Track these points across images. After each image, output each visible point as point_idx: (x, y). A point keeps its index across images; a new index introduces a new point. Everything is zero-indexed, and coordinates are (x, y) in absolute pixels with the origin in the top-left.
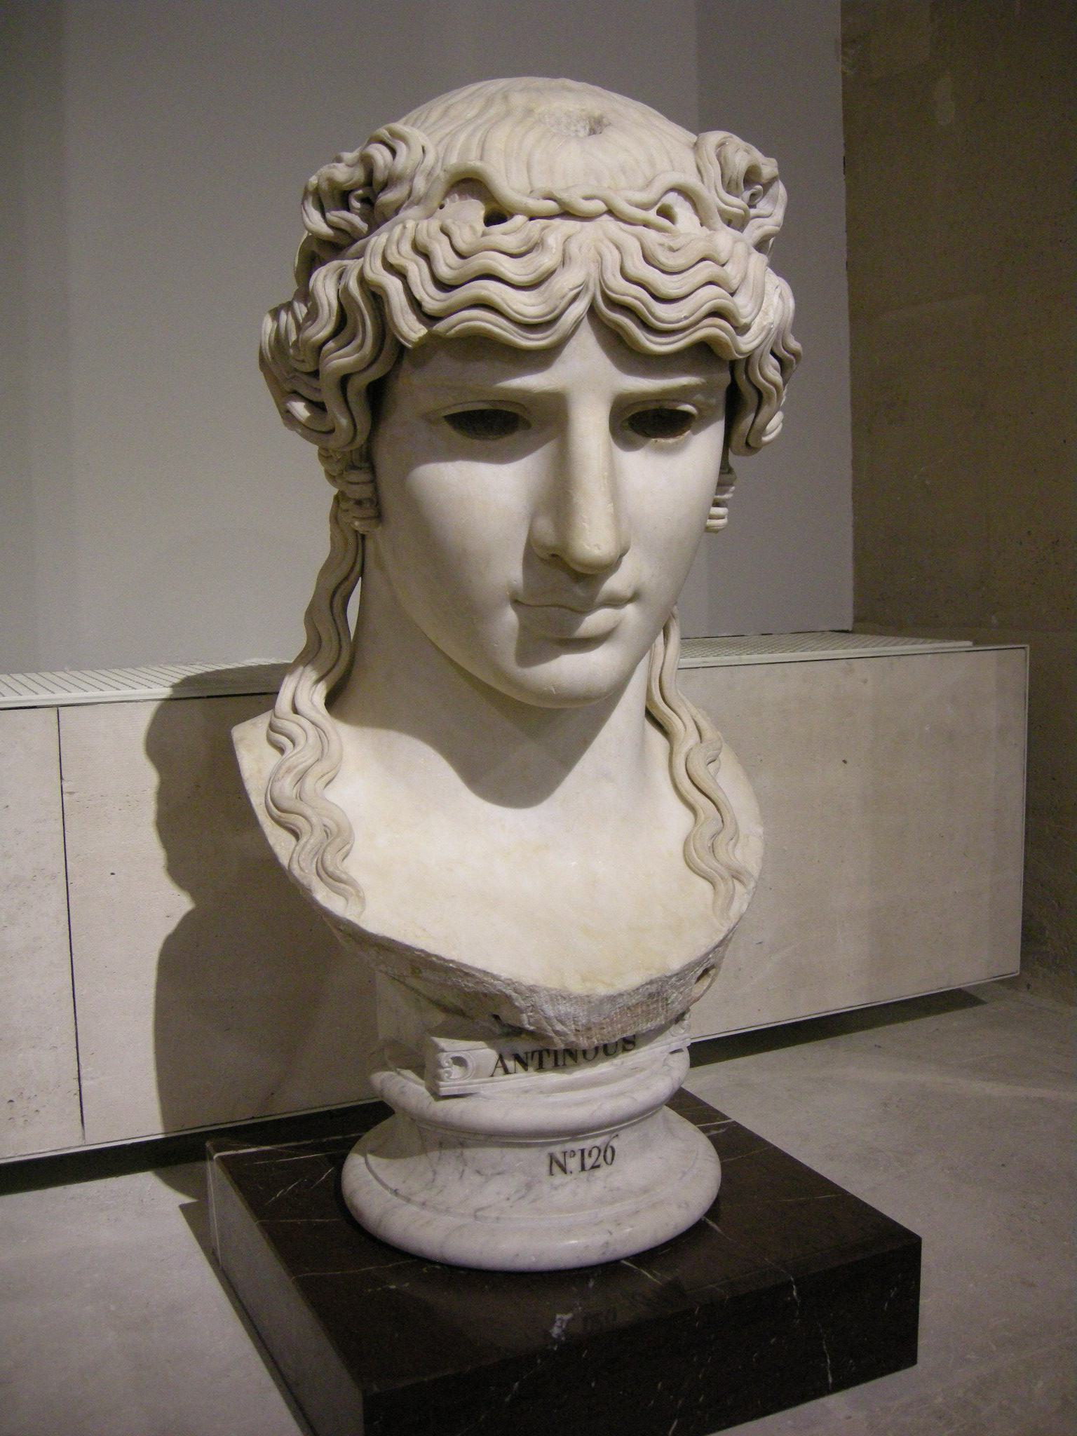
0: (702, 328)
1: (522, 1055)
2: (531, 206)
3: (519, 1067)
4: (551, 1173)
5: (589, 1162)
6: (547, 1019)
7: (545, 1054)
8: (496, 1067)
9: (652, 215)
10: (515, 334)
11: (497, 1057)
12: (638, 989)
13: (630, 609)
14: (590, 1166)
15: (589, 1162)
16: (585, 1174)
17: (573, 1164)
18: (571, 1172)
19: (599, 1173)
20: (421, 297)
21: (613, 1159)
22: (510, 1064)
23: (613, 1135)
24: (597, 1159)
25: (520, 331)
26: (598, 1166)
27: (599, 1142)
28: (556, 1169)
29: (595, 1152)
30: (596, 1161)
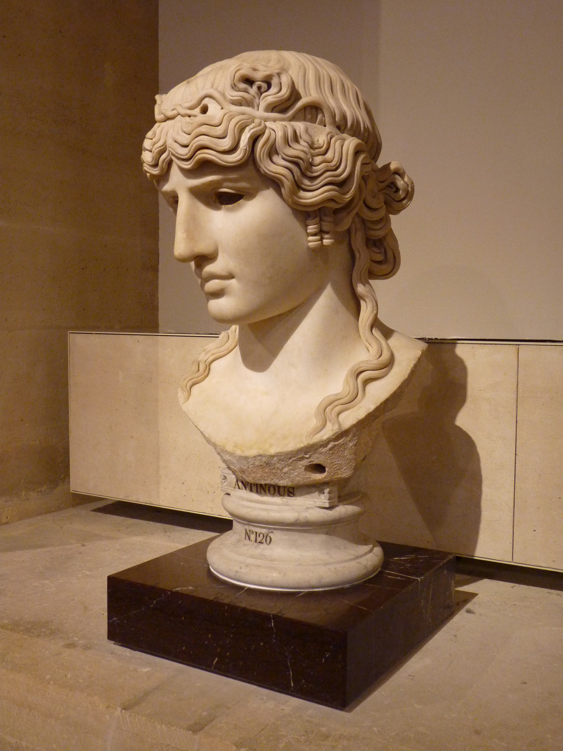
0: (198, 155)
1: (245, 483)
3: (243, 488)
4: (245, 539)
5: (259, 539)
7: (253, 486)
8: (235, 484)
9: (197, 111)
11: (236, 480)
12: (254, 457)
13: (233, 282)
14: (259, 541)
15: (259, 539)
16: (256, 544)
17: (253, 537)
18: (251, 541)
19: (262, 546)
21: (270, 543)
22: (240, 484)
23: (270, 531)
24: (262, 539)
25: (152, 168)
26: (262, 543)
27: (264, 531)
28: (247, 537)
29: (261, 535)
30: (261, 540)
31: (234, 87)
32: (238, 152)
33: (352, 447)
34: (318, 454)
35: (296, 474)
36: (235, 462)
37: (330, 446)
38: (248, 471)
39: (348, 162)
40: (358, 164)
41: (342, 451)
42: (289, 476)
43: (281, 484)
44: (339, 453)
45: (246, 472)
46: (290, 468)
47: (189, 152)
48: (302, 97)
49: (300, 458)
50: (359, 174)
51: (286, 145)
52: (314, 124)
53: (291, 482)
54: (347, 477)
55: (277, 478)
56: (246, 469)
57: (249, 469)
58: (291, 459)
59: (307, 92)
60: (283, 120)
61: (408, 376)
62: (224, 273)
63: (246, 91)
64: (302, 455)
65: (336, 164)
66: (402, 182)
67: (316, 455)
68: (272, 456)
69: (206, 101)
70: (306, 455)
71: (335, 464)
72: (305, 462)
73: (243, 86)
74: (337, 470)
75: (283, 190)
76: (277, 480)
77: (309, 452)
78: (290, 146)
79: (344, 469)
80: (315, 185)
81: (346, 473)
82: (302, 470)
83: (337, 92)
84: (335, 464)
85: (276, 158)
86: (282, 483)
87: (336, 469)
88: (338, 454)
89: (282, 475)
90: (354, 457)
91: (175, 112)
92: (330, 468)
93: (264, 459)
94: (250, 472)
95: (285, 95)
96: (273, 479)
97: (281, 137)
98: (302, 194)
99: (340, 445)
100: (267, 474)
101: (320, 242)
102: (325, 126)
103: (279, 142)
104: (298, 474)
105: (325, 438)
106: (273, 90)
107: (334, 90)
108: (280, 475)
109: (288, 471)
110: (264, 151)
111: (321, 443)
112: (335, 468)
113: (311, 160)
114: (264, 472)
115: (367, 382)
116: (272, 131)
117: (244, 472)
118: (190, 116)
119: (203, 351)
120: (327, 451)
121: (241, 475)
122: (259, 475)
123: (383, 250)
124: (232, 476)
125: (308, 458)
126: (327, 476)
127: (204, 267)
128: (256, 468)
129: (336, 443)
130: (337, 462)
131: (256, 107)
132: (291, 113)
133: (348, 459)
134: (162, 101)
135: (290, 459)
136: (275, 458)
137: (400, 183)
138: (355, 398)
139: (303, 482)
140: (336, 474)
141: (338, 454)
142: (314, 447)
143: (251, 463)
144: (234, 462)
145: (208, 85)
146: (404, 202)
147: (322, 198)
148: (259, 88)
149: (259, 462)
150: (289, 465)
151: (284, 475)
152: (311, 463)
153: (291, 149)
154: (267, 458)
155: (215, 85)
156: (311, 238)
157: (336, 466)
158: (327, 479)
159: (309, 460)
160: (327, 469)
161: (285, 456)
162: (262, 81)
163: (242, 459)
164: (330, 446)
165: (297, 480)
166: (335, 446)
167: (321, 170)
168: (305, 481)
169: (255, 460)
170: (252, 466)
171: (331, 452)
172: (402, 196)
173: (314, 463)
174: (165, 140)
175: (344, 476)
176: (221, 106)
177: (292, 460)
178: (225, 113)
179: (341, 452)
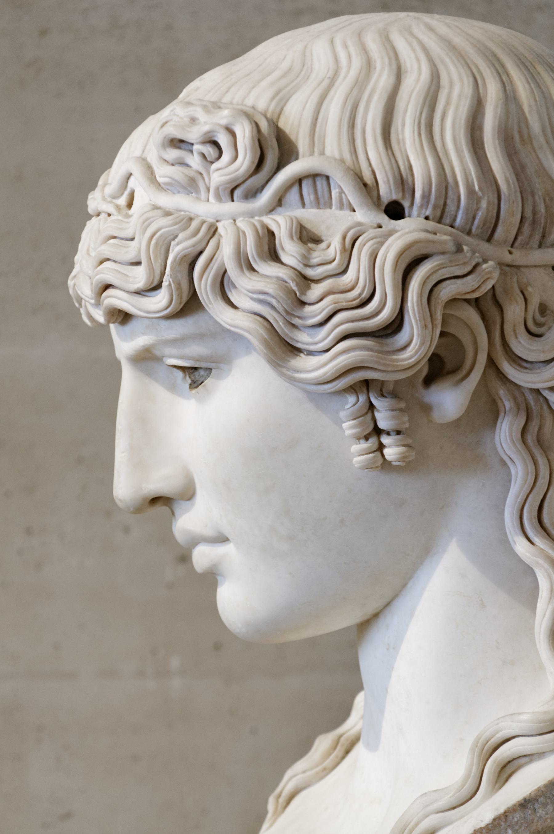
40: (414, 286)
50: (416, 308)
51: (242, 269)
52: (329, 210)
78: (252, 269)
83: (403, 125)
102: (354, 211)
106: (226, 157)
147: (334, 367)
148: (204, 156)
153: (253, 276)
162: (204, 143)
167: (323, 310)
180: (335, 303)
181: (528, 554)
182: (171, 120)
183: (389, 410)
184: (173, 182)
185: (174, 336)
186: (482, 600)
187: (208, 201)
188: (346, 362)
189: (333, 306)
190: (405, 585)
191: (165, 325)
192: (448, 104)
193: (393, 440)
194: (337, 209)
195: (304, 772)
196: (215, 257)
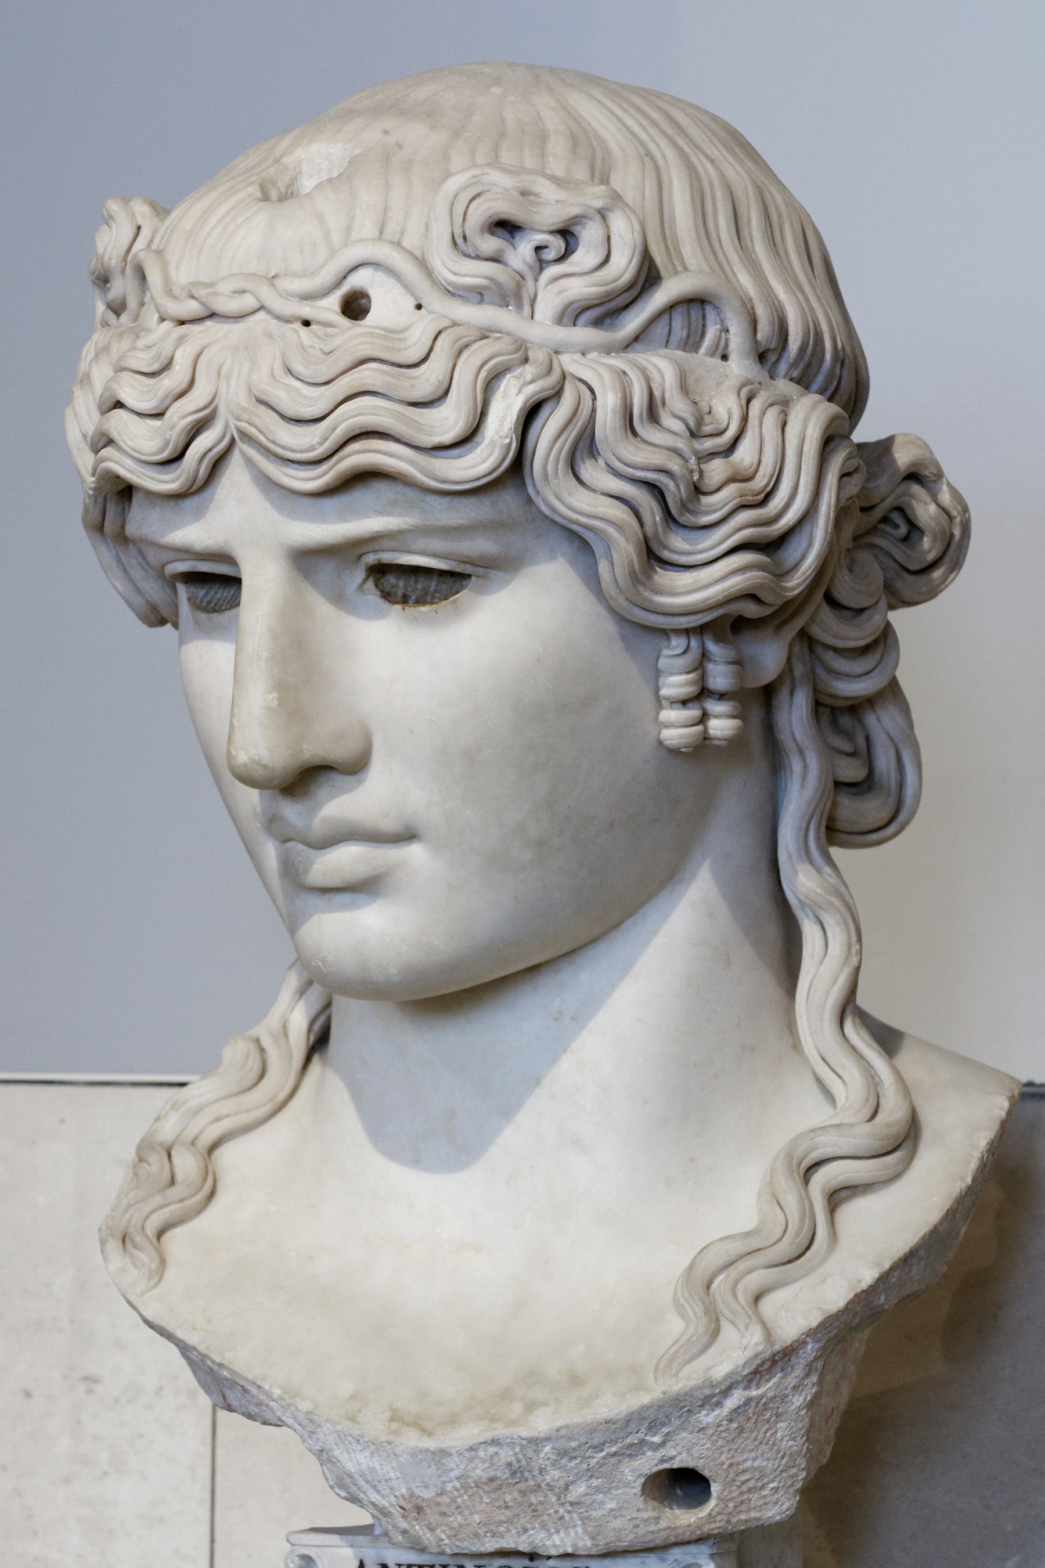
2: (169, 311)
6: (350, 1476)
10: (142, 476)
12: (471, 1449)
13: (415, 852)
20: (86, 430)
31: (459, 244)
32: (479, 449)
33: (800, 1408)
34: (691, 1433)
35: (611, 1505)
36: (392, 1475)
37: (732, 1402)
38: (439, 1504)
39: (802, 476)
41: (768, 1421)
42: (586, 1514)
43: (555, 1546)
44: (759, 1431)
45: (429, 1512)
46: (595, 1482)
47: (321, 444)
48: (663, 272)
49: (631, 1445)
52: (695, 354)
53: (593, 1538)
54: (778, 1518)
55: (544, 1526)
56: (429, 1500)
57: (445, 1499)
58: (602, 1450)
59: (672, 251)
60: (608, 349)
61: (974, 1179)
62: (389, 825)
63: (496, 259)
64: (640, 1435)
65: (766, 486)
66: (933, 508)
67: (684, 1434)
68: (536, 1442)
69: (359, 280)
70: (655, 1435)
71: (744, 1471)
72: (649, 1463)
73: (491, 244)
74: (749, 1491)
75: (603, 568)
76: (542, 1535)
77: (664, 1425)
78: (634, 433)
79: (772, 1489)
80: (701, 552)
81: (776, 1503)
82: (634, 1491)
84: (744, 1471)
85: (589, 471)
86: (558, 1543)
87: (744, 1488)
88: (754, 1435)
89: (561, 1511)
90: (805, 1447)
91: (248, 302)
92: (728, 1484)
93: (506, 1455)
94: (444, 1510)
95: (622, 276)
96: (526, 1530)
97: (614, 411)
98: (664, 577)
99: (764, 1400)
100: (507, 1513)
101: (700, 728)
102: (725, 357)
103: (606, 425)
104: (620, 1508)
105: (720, 1372)
106: (585, 257)
107: (745, 233)
108: (556, 1512)
109: (586, 1494)
110: (561, 450)
111: (707, 1392)
112: (743, 1483)
113: (696, 477)
114: (497, 1504)
115: (837, 1197)
116: (583, 388)
117: (419, 1509)
118: (307, 323)
119: (171, 1108)
120: (721, 1421)
121: (404, 1525)
122: (477, 1518)
123: (861, 741)
124: (338, 1550)
125: (657, 1447)
126: (714, 1513)
127: (320, 806)
128: (471, 1491)
129: (754, 1393)
130: (750, 1462)
131: (527, 309)
132: (633, 322)
133: (783, 1457)
134: (139, 228)
135: (599, 1447)
136: (548, 1448)
137: (925, 511)
138: (808, 1248)
139: (632, 1536)
140: (744, 1507)
141: (754, 1435)
142: (682, 1404)
143: (453, 1474)
144: (387, 1477)
145: (366, 227)
146: (937, 574)
147: (724, 591)
148: (538, 249)
149: (486, 1465)
150: (591, 1473)
151: (569, 1512)
152: (667, 1466)
154: (518, 1449)
155: (391, 229)
156: (670, 714)
157: (747, 1476)
158: (713, 1526)
159: (659, 1455)
160: (715, 1488)
161: (583, 1439)
162: (552, 232)
163: (421, 1461)
164: (732, 1402)
165: (614, 1529)
166: (748, 1401)
168: (640, 1531)
169: (472, 1460)
170: (457, 1484)
171: (734, 1425)
172: (931, 557)
173: (675, 1466)
174: (214, 391)
175: (770, 1514)
176: (416, 298)
177: (604, 1453)
178: (438, 330)
179: (767, 1426)
180: (741, 496)
181: (819, 891)
182: (489, 191)
183: (725, 662)
184: (492, 286)
185: (461, 521)
186: (728, 954)
187: (532, 318)
188: (742, 585)
189: (739, 499)
190: (616, 926)
191: (440, 504)
192: (780, 216)
193: (731, 708)
194: (706, 354)
195: (181, 1201)
196: (580, 408)
